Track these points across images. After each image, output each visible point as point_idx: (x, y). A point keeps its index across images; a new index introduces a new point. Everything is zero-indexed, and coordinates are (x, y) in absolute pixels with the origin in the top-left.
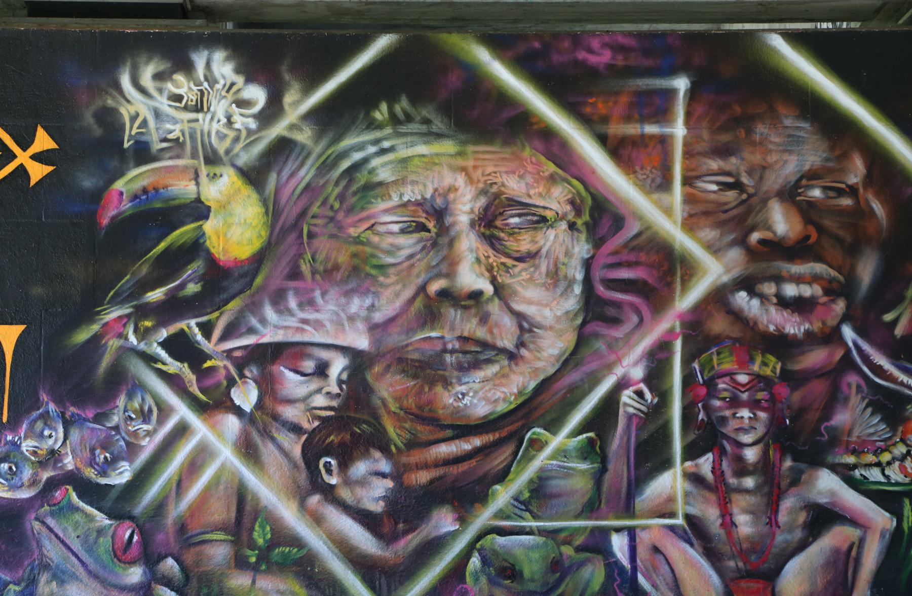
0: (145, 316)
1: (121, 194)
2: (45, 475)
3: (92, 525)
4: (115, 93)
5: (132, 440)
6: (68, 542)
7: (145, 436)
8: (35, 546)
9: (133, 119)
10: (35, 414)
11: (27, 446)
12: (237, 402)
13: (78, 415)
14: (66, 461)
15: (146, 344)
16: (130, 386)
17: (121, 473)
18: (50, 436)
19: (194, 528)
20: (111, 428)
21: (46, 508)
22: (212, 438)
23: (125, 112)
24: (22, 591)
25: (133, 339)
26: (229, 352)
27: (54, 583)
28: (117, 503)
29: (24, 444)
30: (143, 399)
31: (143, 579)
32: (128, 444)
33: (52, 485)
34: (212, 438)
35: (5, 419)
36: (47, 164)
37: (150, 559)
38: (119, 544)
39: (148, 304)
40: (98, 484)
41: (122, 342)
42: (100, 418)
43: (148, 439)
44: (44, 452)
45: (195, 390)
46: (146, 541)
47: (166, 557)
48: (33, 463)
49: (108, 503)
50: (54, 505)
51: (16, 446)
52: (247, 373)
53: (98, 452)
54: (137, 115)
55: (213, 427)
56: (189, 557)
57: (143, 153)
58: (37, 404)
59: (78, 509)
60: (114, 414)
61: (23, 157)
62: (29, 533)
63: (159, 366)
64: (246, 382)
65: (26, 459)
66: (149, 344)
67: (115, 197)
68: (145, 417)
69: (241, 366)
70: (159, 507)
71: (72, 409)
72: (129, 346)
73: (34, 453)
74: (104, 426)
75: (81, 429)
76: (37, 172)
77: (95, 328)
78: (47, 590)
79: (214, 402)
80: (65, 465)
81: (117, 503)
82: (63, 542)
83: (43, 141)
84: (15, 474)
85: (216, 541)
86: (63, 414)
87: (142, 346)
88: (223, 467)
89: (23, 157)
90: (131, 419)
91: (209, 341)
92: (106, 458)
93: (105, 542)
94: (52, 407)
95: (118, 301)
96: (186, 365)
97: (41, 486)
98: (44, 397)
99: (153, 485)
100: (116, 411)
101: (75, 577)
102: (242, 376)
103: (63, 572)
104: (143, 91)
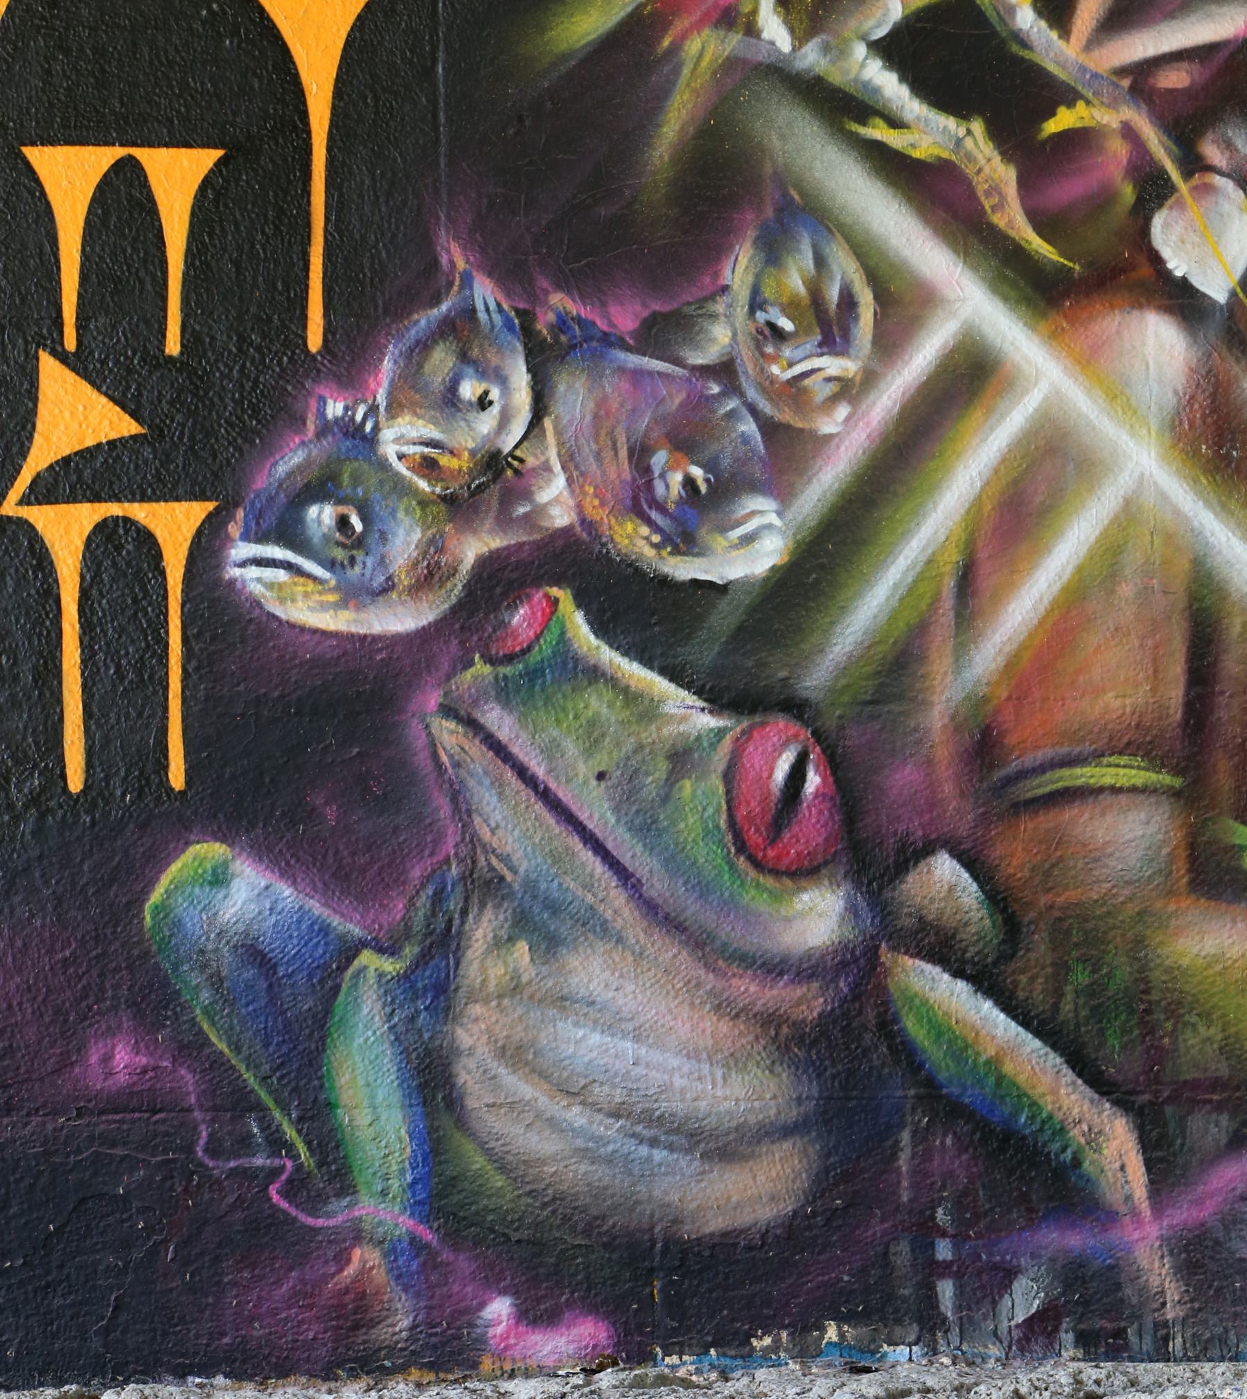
2: (472, 549)
3: (649, 734)
5: (786, 416)
6: (563, 794)
7: (834, 399)
8: (445, 811)
10: (425, 319)
11: (401, 437)
12: (1177, 265)
13: (579, 320)
14: (543, 497)
15: (826, 49)
16: (769, 212)
17: (749, 539)
18: (483, 403)
19: (1027, 745)
20: (707, 371)
21: (481, 668)
22: (1083, 402)
24: (405, 978)
26: (1140, 75)
27: (522, 947)
28: (750, 654)
29: (387, 434)
30: (820, 261)
31: (849, 934)
32: (769, 428)
33: (497, 583)
34: (1083, 402)
35: (315, 340)
37: (871, 857)
38: (750, 806)
40: (665, 582)
41: (734, 41)
42: (662, 334)
43: (842, 411)
44: (462, 463)
45: (1013, 220)
46: (849, 796)
47: (928, 850)
48: (423, 503)
49: (703, 653)
50: (510, 659)
51: (360, 439)
52: (1212, 152)
53: (660, 459)
55: (1088, 362)
56: (1015, 853)
58: (428, 282)
59: (596, 674)
60: (713, 317)
62: (422, 760)
63: (878, 131)
64: (1208, 189)
65: (401, 488)
66: (838, 51)
68: (831, 328)
69: (1188, 123)
70: (896, 667)
71: (558, 300)
72: (762, 56)
74: (678, 362)
75: (595, 377)
78: (496, 972)
79: (1089, 265)
80: (541, 510)
82: (546, 796)
84: (359, 542)
85: (1115, 790)
86: (526, 317)
87: (811, 57)
88: (1129, 515)
91: (1065, 33)
92: (689, 482)
93: (702, 796)
94: (484, 292)
96: (977, 126)
97: (457, 587)
98: (455, 255)
99: (867, 581)
100: (719, 307)
101: (594, 925)
102: (1193, 164)
103: (554, 908)
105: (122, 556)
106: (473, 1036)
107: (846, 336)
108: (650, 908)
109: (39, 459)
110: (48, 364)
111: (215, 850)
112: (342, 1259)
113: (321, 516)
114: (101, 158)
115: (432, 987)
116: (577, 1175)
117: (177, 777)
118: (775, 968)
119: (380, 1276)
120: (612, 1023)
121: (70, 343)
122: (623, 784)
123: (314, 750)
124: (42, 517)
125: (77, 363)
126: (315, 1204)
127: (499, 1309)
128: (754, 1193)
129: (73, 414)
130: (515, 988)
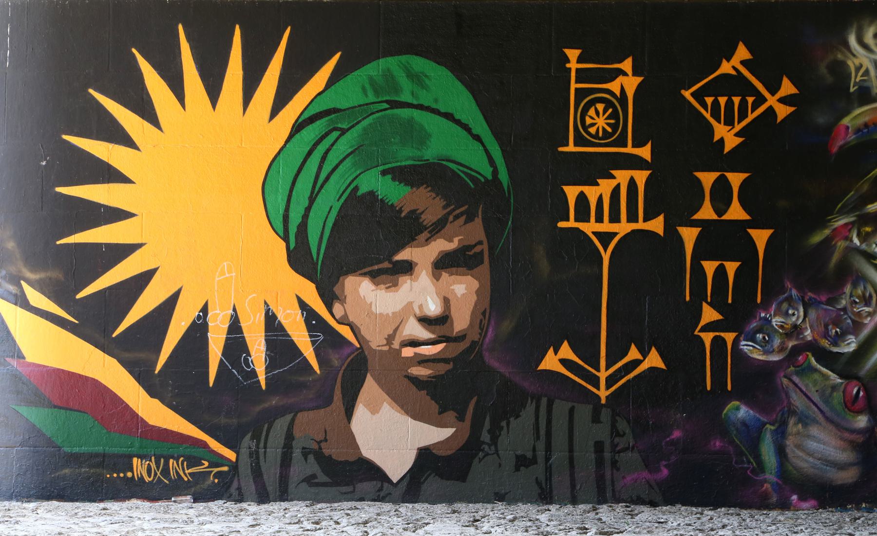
0: (866, 225)
1: (848, 128)
2: (791, 344)
3: (827, 383)
4: (844, 49)
5: (857, 319)
8: (784, 397)
9: (858, 69)
11: (776, 321)
14: (806, 334)
15: (867, 245)
17: (849, 344)
18: (794, 314)
21: (792, 368)
23: (851, 64)
24: (776, 430)
25: (856, 241)
28: (848, 367)
29: (774, 320)
32: (853, 321)
33: (796, 351)
35: (759, 301)
36: (790, 105)
39: (869, 214)
40: (831, 352)
41: (848, 243)
42: (832, 301)
43: (869, 319)
48: (781, 334)
50: (798, 366)
53: (830, 327)
54: (861, 66)
57: (865, 95)
58: (783, 290)
61: (772, 101)
66: (870, 245)
67: (843, 130)
73: (782, 327)
76: (783, 112)
77: (827, 232)
78: (795, 430)
81: (848, 367)
82: (805, 395)
83: (787, 88)
84: (767, 342)
86: (803, 298)
87: (864, 246)
89: (772, 101)
90: (856, 303)
92: (836, 332)
93: (838, 396)
94: (794, 292)
95: (843, 212)
98: (788, 285)
101: (815, 421)
103: (807, 417)
104: (866, 47)
105: (719, 343)
106: (790, 442)
107: (870, 303)
108: (827, 418)
109: (702, 323)
110: (704, 304)
111: (737, 403)
112: (763, 486)
113: (760, 336)
114: (716, 264)
115: (781, 433)
116: (811, 471)
117: (729, 388)
118: (853, 431)
119: (770, 489)
120: (819, 441)
121: (709, 300)
122: (822, 393)
123: (757, 383)
124: (702, 335)
125: (710, 304)
126: (757, 475)
127: (795, 497)
128: (848, 476)
129: (709, 314)
130: (798, 433)
